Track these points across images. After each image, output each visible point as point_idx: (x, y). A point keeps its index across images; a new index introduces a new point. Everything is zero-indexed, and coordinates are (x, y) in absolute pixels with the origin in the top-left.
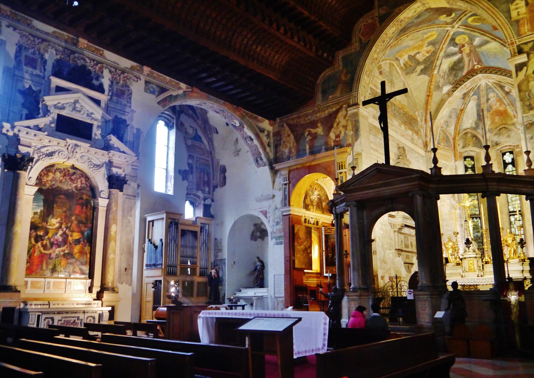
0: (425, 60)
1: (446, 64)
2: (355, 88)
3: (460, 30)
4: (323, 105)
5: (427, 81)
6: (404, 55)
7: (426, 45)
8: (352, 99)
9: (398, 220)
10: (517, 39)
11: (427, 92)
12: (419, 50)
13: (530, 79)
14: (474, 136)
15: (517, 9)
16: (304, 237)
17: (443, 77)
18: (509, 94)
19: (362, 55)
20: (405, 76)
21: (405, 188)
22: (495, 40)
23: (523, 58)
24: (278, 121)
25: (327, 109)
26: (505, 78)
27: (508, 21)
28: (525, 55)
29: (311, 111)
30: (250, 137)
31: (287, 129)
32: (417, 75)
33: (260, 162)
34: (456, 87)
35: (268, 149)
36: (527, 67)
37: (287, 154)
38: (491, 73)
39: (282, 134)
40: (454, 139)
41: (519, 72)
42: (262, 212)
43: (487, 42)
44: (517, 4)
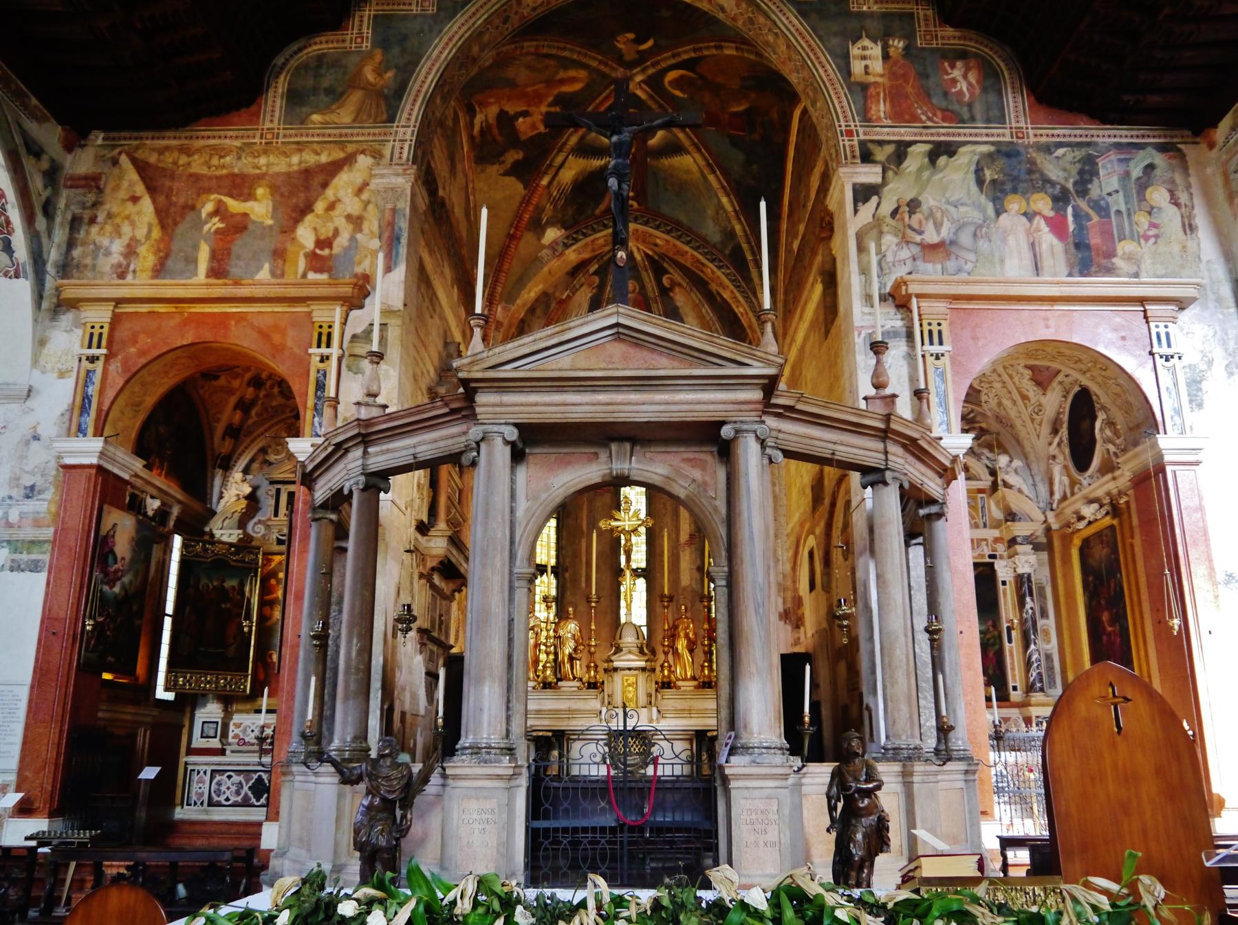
0: (532, 138)
1: (571, 170)
2: (405, 115)
3: (639, 93)
4: (285, 136)
5: (518, 199)
6: (491, 104)
7: (550, 99)
8: (392, 143)
9: (432, 544)
10: (861, 126)
11: (511, 226)
12: (529, 105)
13: (885, 229)
15: (864, 58)
16: (128, 556)
17: (555, 203)
18: (668, 295)
19: (440, 31)
20: (473, 165)
21: (711, 407)
22: (699, 150)
23: (870, 174)
24: (100, 142)
25: (300, 151)
26: (686, 248)
27: (844, 80)
28: (879, 169)
29: (237, 143)
31: (132, 175)
32: (501, 171)
34: (574, 239)
35: (41, 223)
36: (880, 198)
37: (116, 258)
38: (657, 228)
39: (108, 191)
41: (860, 204)
43: (674, 149)
44: (864, 48)
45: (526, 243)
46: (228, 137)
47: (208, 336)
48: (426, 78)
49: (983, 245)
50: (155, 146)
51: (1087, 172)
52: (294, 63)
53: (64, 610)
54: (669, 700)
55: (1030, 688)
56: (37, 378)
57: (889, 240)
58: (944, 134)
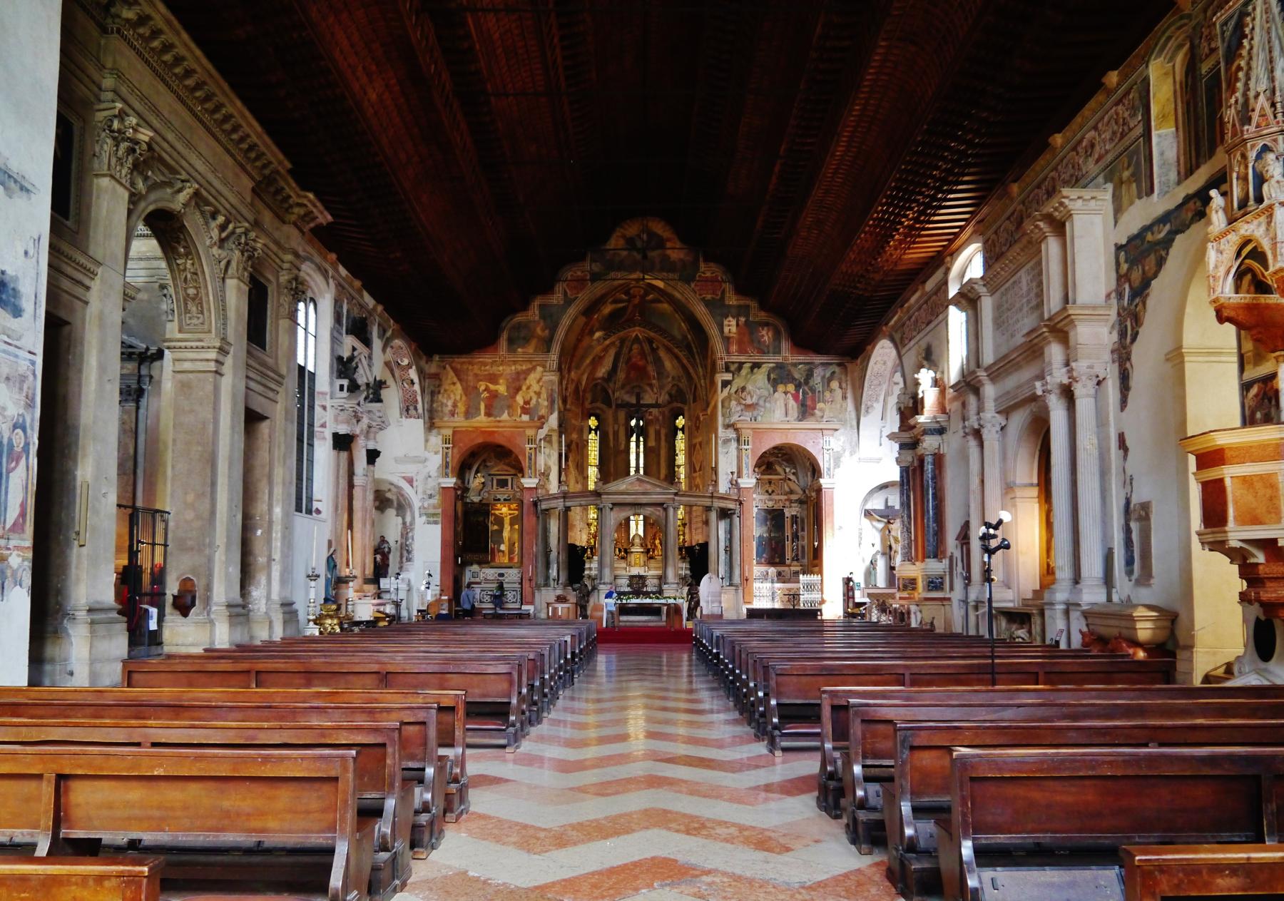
1: (607, 309)
14: (605, 391)
23: (728, 377)
30: (412, 381)
31: (451, 373)
33: (412, 412)
40: (584, 391)
42: (404, 478)
43: (660, 301)
45: (586, 341)
46: (487, 358)
47: (489, 439)
48: (560, 333)
49: (768, 405)
50: (459, 361)
51: (809, 375)
52: (509, 326)
53: (450, 537)
54: (652, 563)
55: (793, 560)
56: (427, 454)
57: (733, 403)
58: (757, 359)
